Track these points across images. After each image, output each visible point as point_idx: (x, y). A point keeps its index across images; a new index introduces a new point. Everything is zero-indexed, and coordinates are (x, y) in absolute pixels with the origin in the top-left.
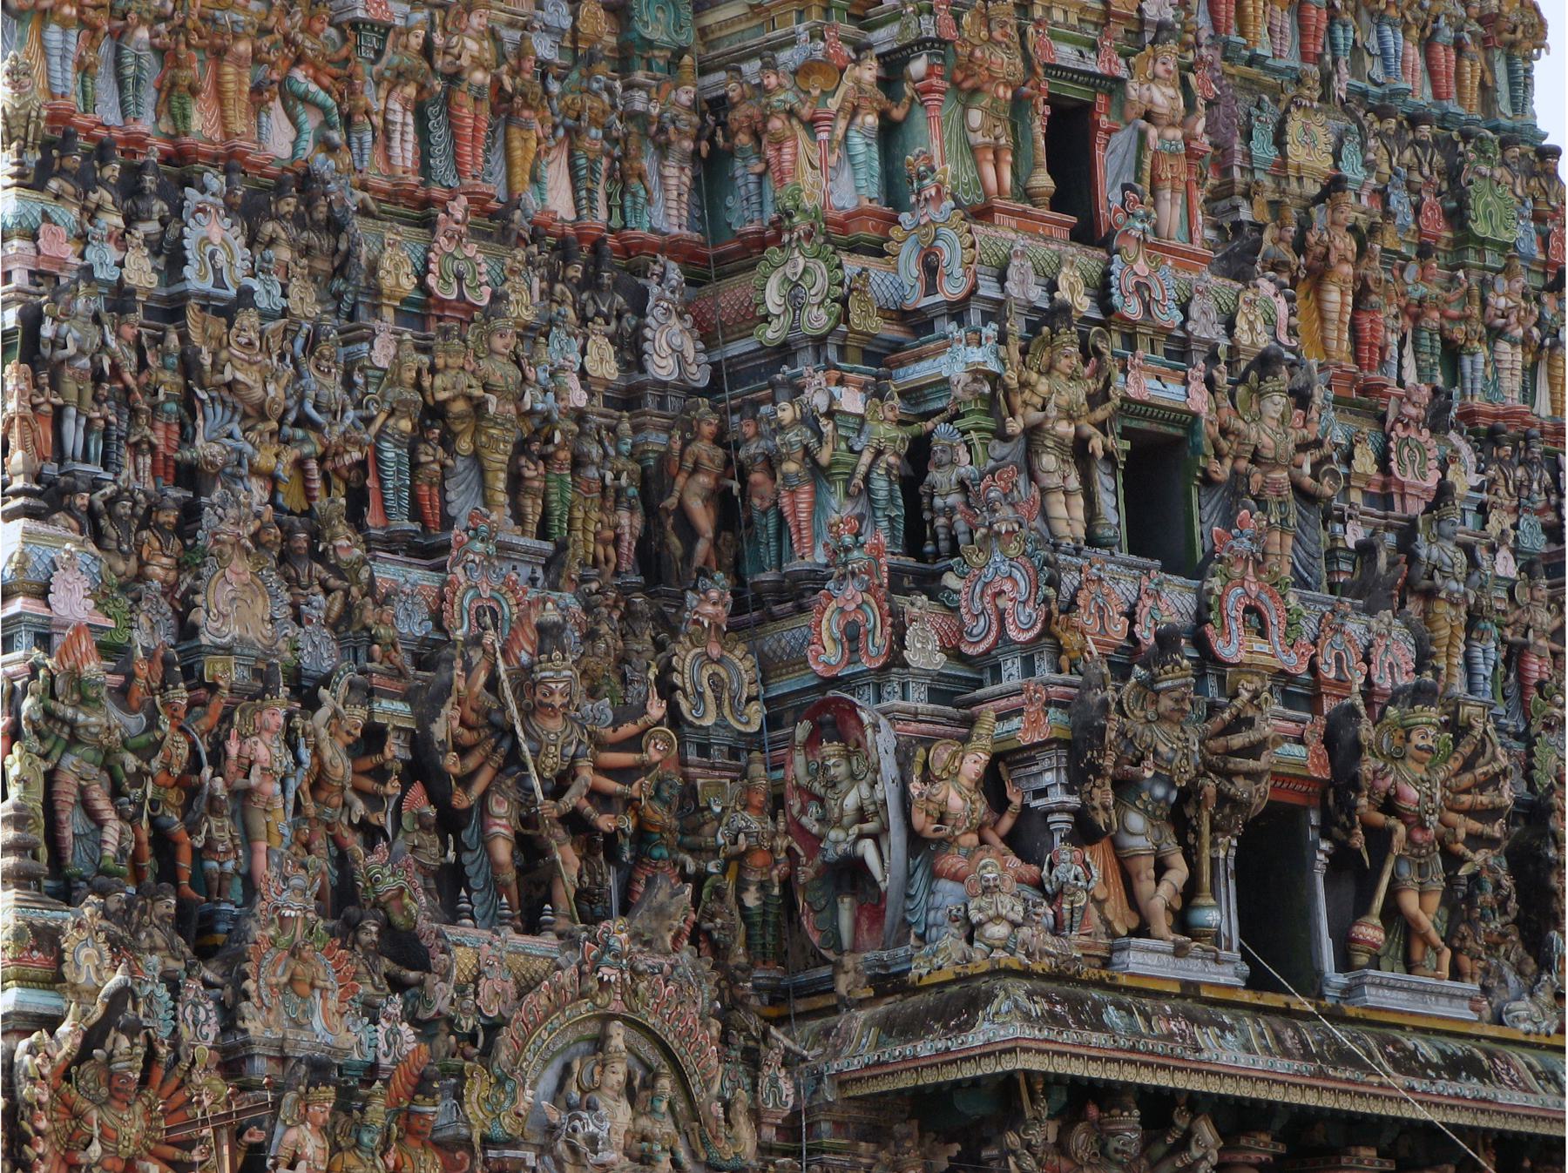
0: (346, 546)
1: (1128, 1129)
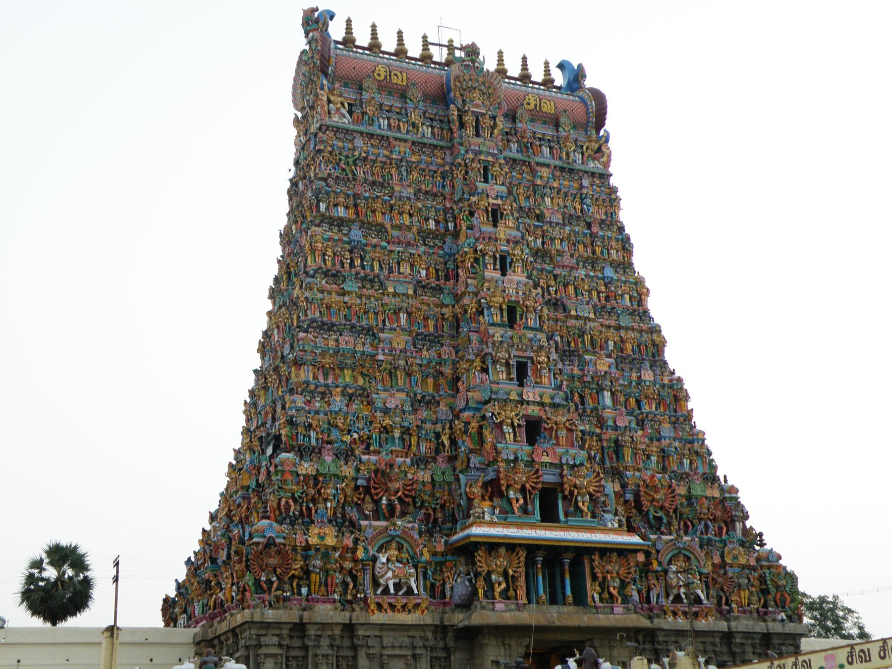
1: (502, 551)
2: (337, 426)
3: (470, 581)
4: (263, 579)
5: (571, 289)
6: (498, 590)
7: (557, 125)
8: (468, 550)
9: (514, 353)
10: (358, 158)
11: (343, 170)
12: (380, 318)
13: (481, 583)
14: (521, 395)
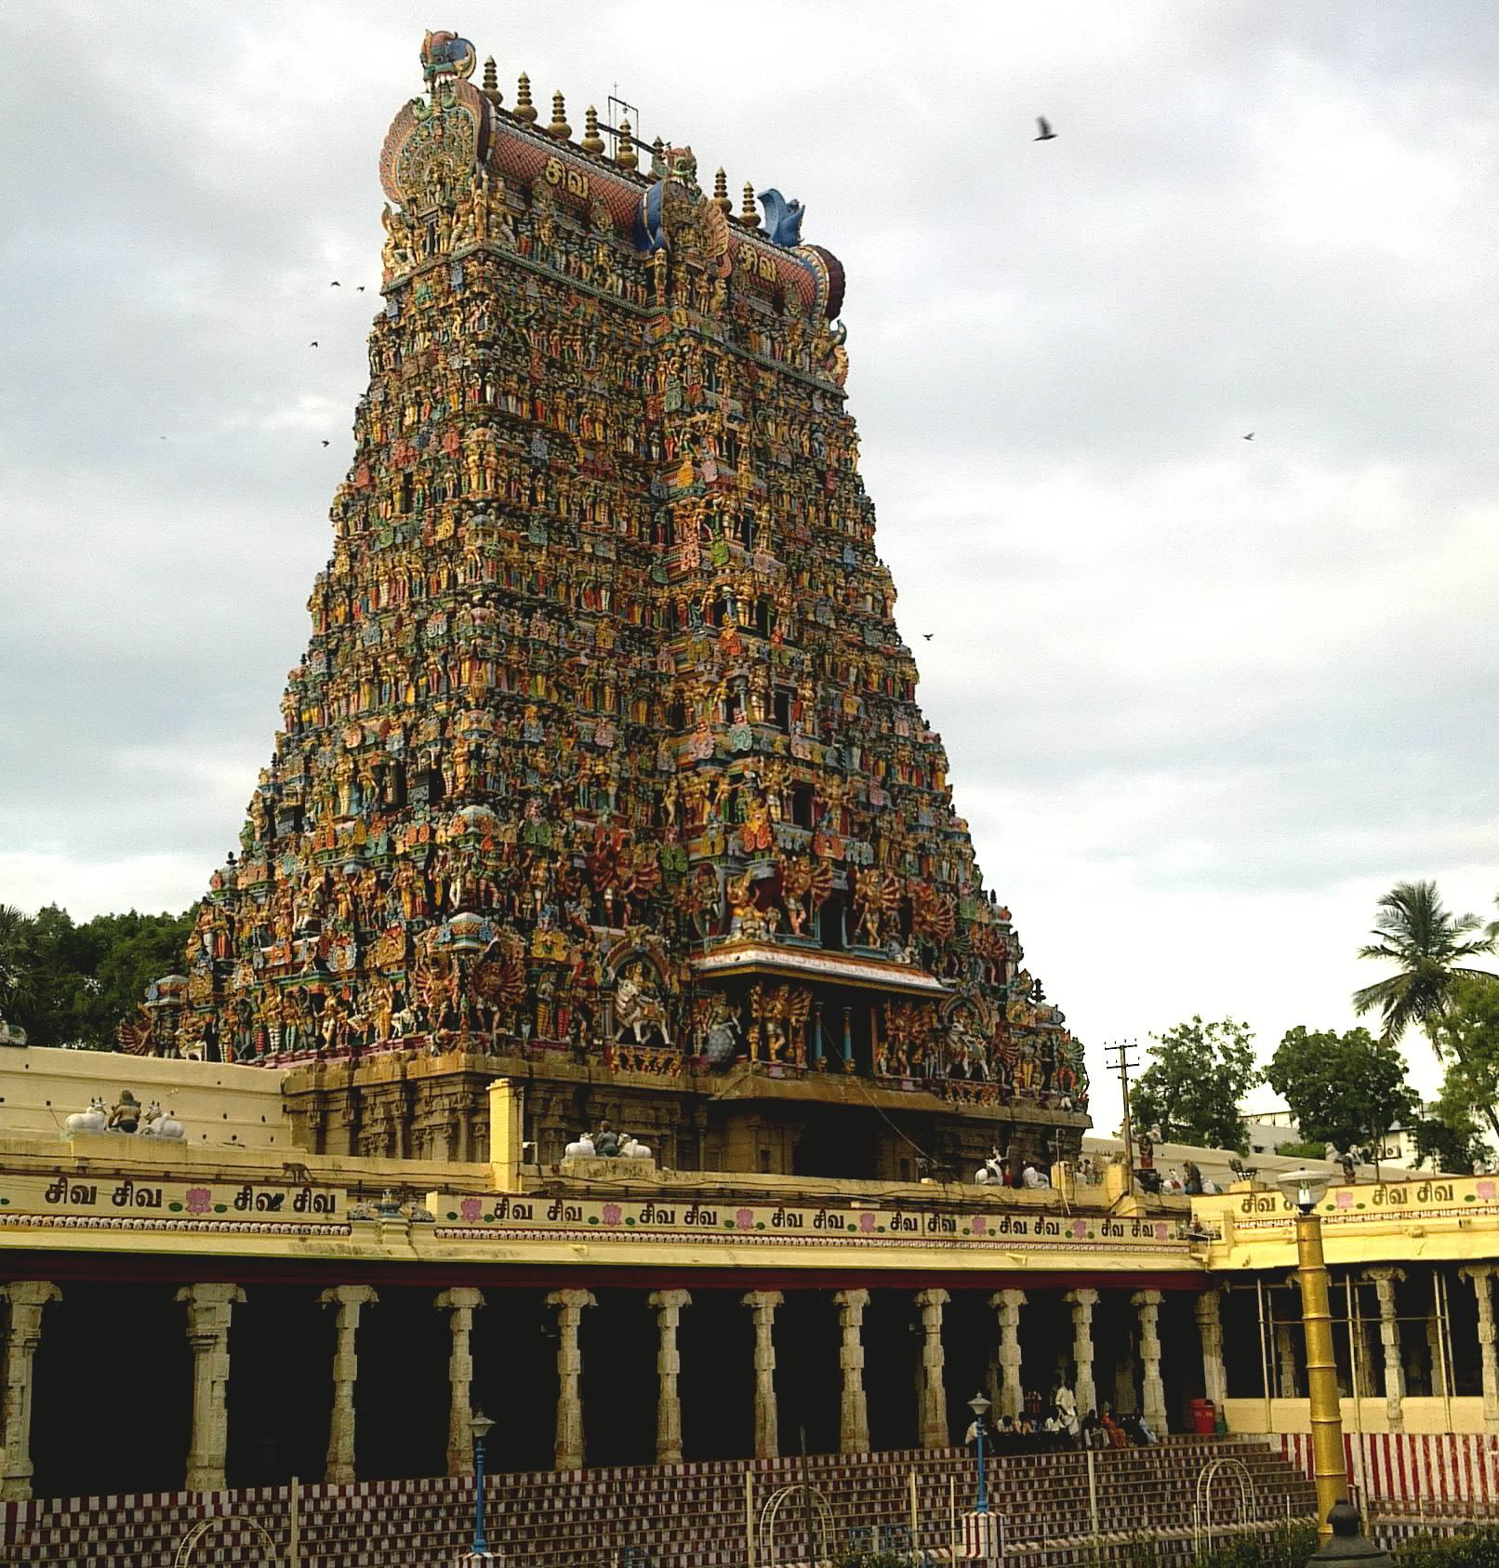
0: (567, 814)
1: (784, 989)
2: (536, 768)
3: (733, 1028)
4: (480, 1006)
5: (806, 576)
6: (775, 1046)
7: (779, 304)
8: (737, 986)
9: (775, 680)
10: (532, 317)
11: (511, 332)
12: (573, 595)
13: (753, 1035)
14: (788, 748)
